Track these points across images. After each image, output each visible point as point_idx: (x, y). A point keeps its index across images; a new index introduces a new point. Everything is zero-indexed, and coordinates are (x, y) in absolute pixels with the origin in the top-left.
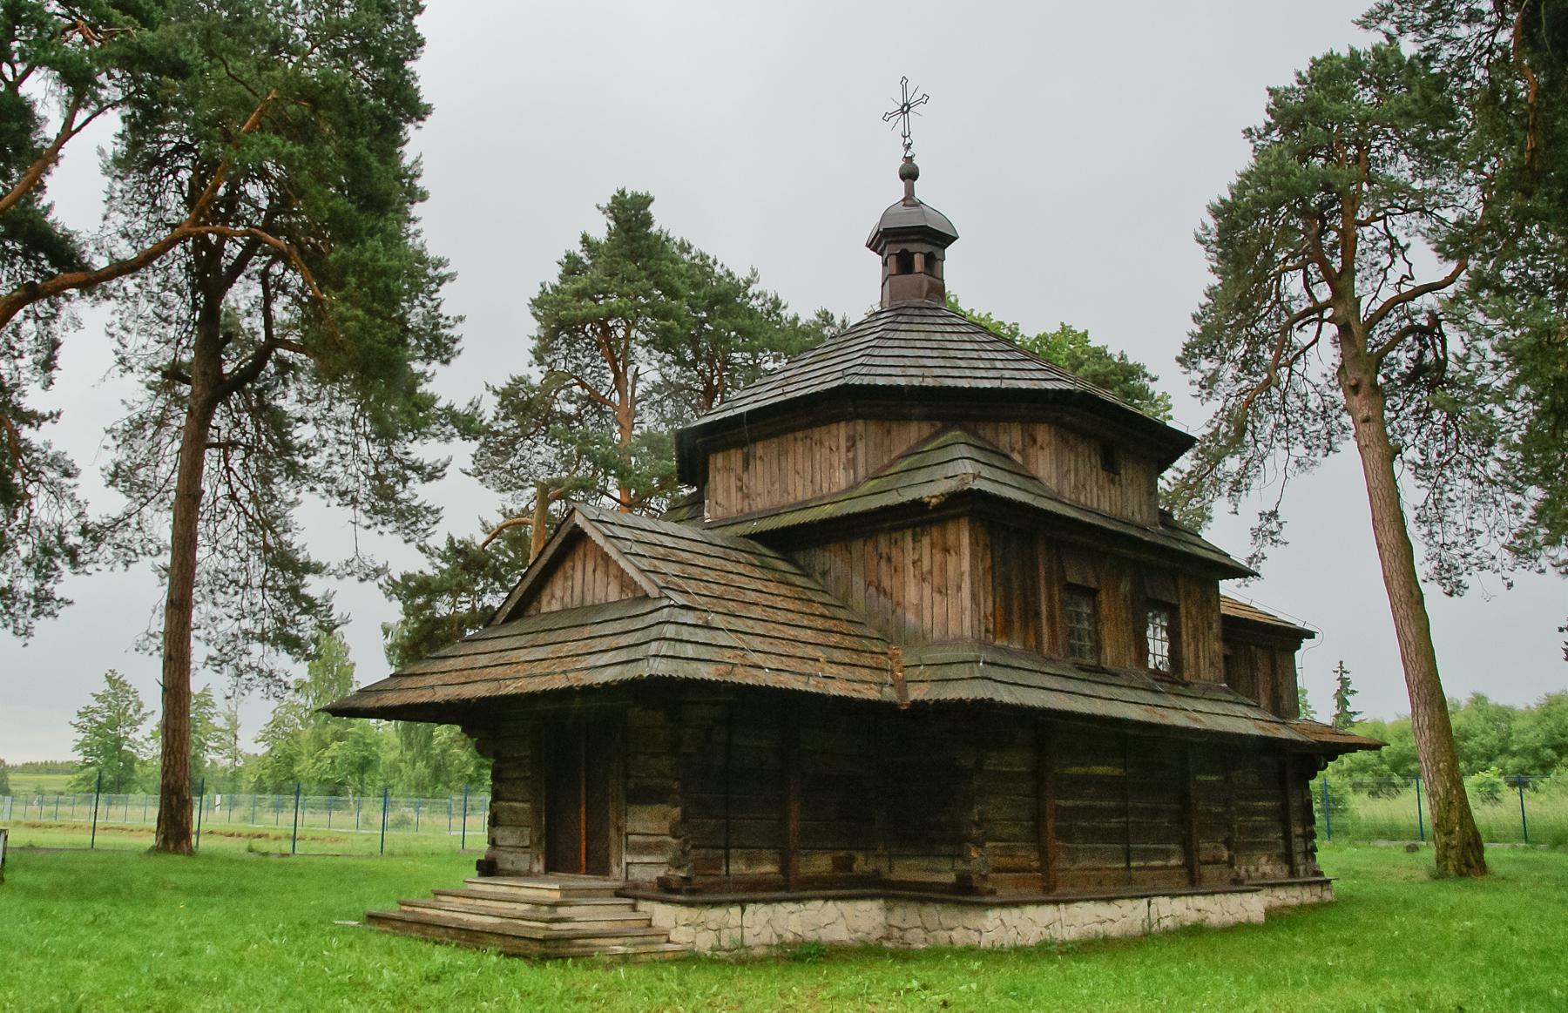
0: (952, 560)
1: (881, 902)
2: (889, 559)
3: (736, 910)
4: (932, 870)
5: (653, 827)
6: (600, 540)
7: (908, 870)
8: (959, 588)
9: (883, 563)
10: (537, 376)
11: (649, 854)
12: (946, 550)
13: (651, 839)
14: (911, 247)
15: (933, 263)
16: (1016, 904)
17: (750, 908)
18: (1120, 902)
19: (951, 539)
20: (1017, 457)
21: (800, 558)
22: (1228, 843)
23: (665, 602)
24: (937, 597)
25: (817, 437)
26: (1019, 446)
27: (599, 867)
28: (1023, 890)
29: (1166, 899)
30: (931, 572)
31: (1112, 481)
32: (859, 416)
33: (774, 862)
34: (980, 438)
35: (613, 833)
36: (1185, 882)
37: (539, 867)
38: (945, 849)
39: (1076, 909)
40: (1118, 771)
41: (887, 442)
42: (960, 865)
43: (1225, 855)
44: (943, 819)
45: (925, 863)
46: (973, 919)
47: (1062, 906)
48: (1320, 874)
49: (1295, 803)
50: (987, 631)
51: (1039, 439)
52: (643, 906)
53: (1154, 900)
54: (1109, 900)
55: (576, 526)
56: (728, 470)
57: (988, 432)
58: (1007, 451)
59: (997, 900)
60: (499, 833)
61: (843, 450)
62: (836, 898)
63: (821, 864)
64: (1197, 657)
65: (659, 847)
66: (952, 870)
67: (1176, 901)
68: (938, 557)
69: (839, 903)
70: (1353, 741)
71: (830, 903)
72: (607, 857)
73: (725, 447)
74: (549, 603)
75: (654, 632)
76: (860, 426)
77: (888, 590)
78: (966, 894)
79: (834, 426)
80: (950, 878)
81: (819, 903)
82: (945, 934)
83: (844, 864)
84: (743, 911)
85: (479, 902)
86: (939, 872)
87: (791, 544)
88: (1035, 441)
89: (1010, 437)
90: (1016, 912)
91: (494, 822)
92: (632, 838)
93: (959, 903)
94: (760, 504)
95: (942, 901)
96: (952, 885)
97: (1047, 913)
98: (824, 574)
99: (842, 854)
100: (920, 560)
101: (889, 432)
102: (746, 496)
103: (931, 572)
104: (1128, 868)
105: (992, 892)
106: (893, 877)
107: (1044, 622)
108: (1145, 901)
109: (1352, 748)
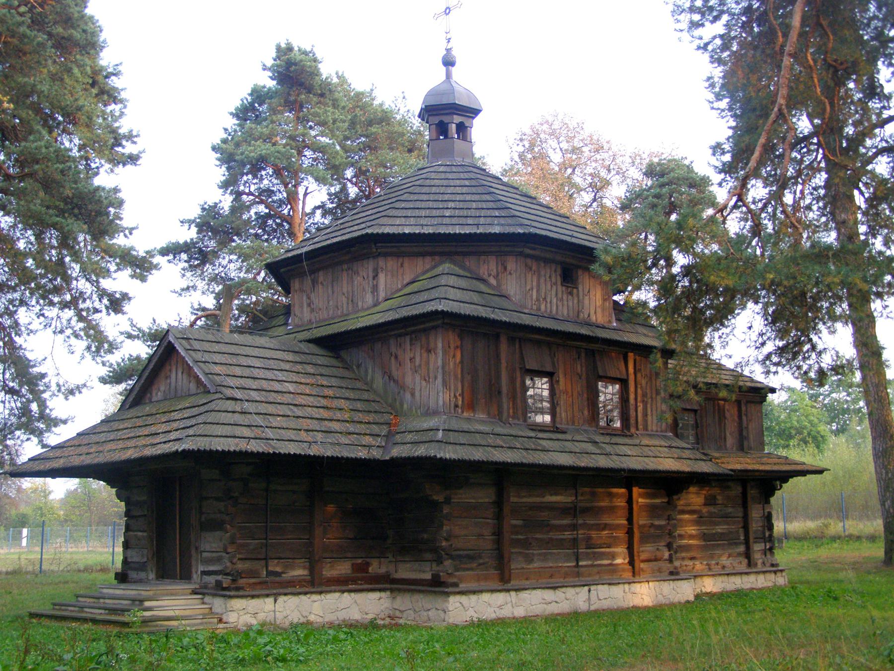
0: (432, 357)
1: (388, 593)
2: (396, 357)
3: (270, 600)
5: (215, 546)
6: (183, 353)
7: (406, 571)
8: (436, 378)
9: (393, 358)
10: (226, 202)
11: (213, 564)
12: (430, 351)
13: (214, 555)
14: (446, 119)
15: (462, 129)
16: (474, 592)
17: (281, 599)
18: (564, 589)
19: (432, 345)
20: (493, 281)
21: (343, 354)
22: (669, 546)
23: (218, 396)
24: (424, 383)
25: (355, 269)
26: (494, 272)
27: (186, 576)
28: (482, 583)
29: (606, 586)
30: (420, 365)
31: (571, 294)
32: (379, 255)
33: (304, 568)
34: (462, 267)
35: (193, 552)
36: (631, 574)
37: (152, 576)
38: (428, 556)
39: (524, 595)
40: (569, 499)
41: (401, 271)
43: (666, 555)
44: (425, 536)
45: (416, 565)
46: (439, 602)
47: (513, 593)
48: (777, 565)
49: (756, 513)
50: (456, 406)
51: (509, 268)
52: (207, 599)
53: (592, 588)
54: (554, 588)
55: (170, 342)
56: (302, 290)
57: (470, 262)
58: (485, 277)
59: (457, 590)
60: (129, 552)
61: (371, 279)
62: (350, 591)
63: (343, 568)
64: (645, 415)
65: (219, 560)
67: (614, 588)
68: (425, 355)
69: (353, 594)
70: (799, 468)
71: (346, 594)
72: (190, 565)
73: (301, 275)
74: (157, 394)
75: (200, 419)
76: (381, 262)
77: (396, 378)
78: (438, 586)
79: (365, 262)
80: (428, 576)
81: (337, 595)
82: (425, 614)
83: (362, 568)
84: (275, 601)
86: (424, 572)
87: (336, 344)
88: (505, 268)
89: (488, 267)
90: (474, 598)
91: (126, 545)
92: (205, 555)
93: (435, 592)
94: (324, 315)
97: (500, 597)
98: (359, 366)
99: (360, 561)
100: (414, 358)
101: (402, 265)
102: (312, 310)
104: (577, 566)
105: (456, 585)
106: (398, 576)
107: (505, 400)
108: (586, 588)
109: (803, 473)
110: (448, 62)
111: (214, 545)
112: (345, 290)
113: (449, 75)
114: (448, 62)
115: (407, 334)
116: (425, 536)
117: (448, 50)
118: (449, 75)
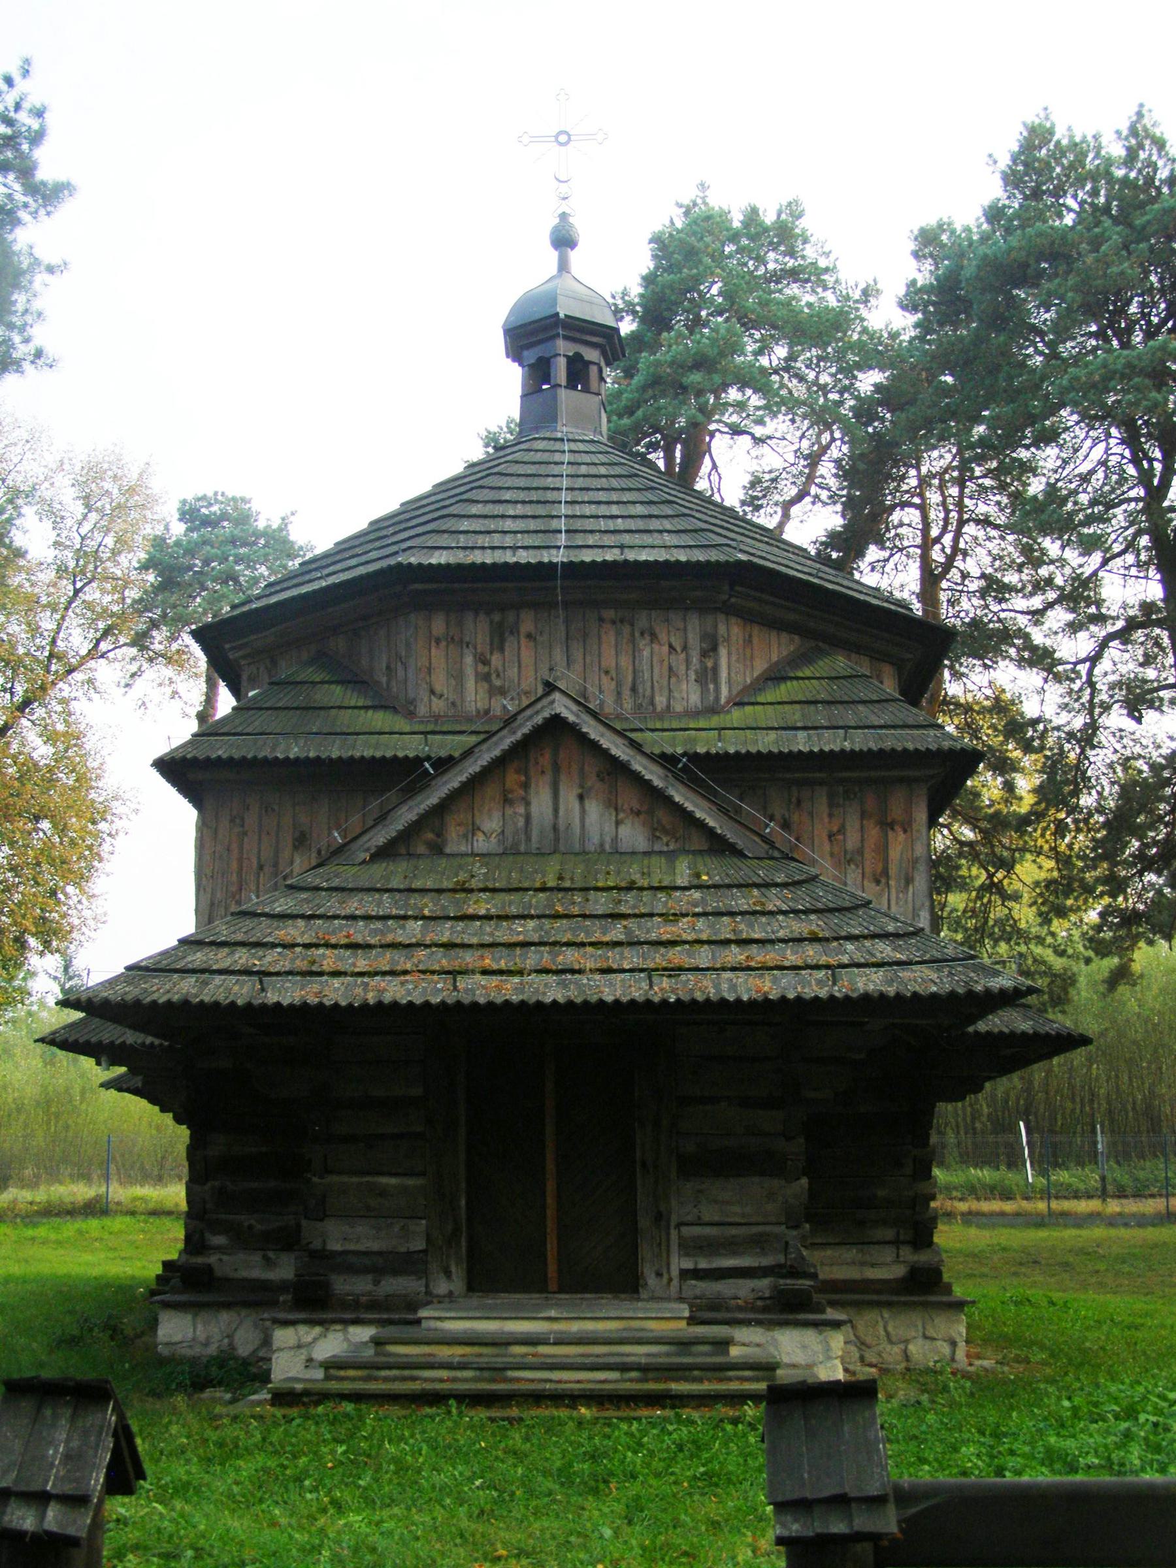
4: (863, 1264)
8: (909, 880)
11: (735, 1254)
12: (887, 825)
13: (734, 1231)
19: (896, 810)
42: (906, 1253)
45: (851, 1253)
56: (459, 642)
65: (759, 1243)
66: (897, 1260)
68: (874, 832)
79: (676, 618)
82: (897, 1349)
85: (542, 1349)
86: (873, 1265)
92: (685, 1230)
95: (889, 1305)
96: (896, 1280)
100: (842, 830)
103: (860, 851)
110: (564, 241)
111: (737, 1209)
112: (609, 660)
113: (563, 266)
114: (564, 241)
115: (821, 783)
116: (881, 1193)
117: (564, 216)
118: (563, 266)
